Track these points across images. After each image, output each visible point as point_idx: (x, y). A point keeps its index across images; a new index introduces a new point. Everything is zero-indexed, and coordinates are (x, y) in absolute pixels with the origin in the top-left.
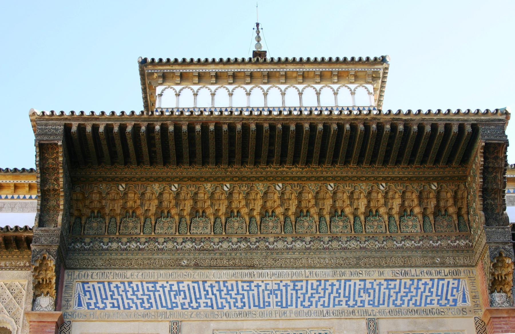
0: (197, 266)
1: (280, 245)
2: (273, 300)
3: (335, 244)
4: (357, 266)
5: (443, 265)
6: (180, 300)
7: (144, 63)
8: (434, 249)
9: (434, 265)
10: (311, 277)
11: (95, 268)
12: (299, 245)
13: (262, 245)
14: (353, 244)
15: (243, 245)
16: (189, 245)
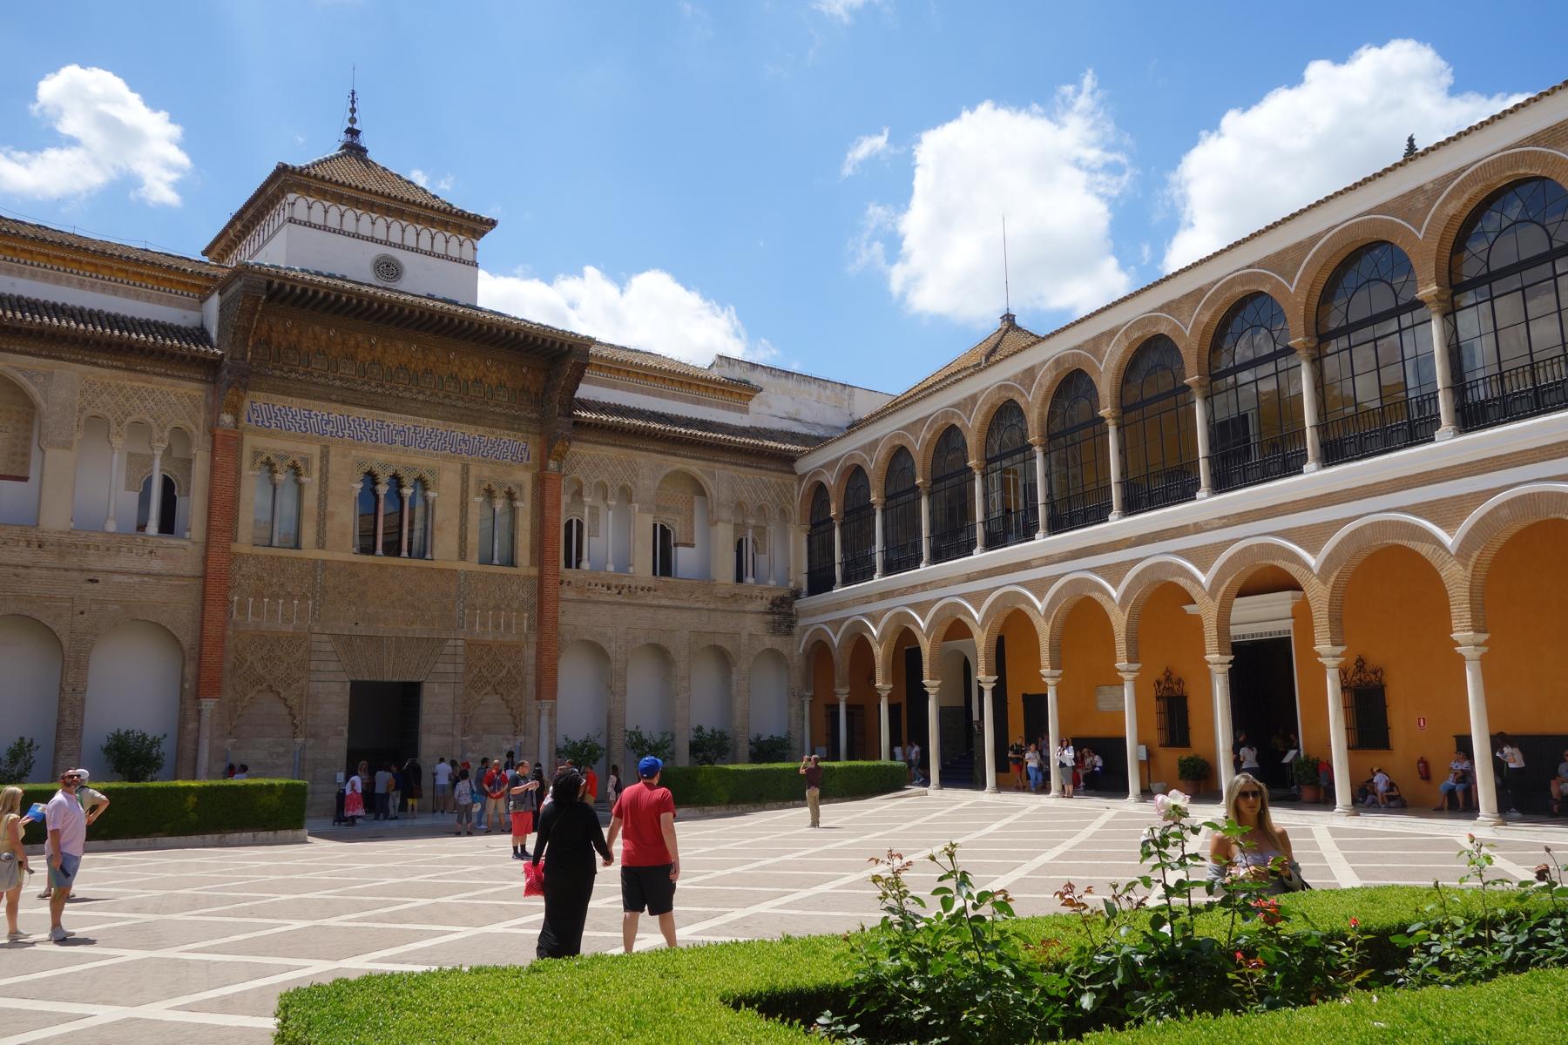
0: (344, 402)
1: (407, 395)
2: (398, 438)
3: (447, 401)
4: (460, 421)
5: (519, 430)
6: (329, 428)
7: (282, 170)
8: (516, 418)
9: (513, 429)
10: (429, 425)
11: (261, 390)
12: (421, 397)
13: (394, 392)
14: (460, 404)
15: (380, 390)
16: (338, 383)
